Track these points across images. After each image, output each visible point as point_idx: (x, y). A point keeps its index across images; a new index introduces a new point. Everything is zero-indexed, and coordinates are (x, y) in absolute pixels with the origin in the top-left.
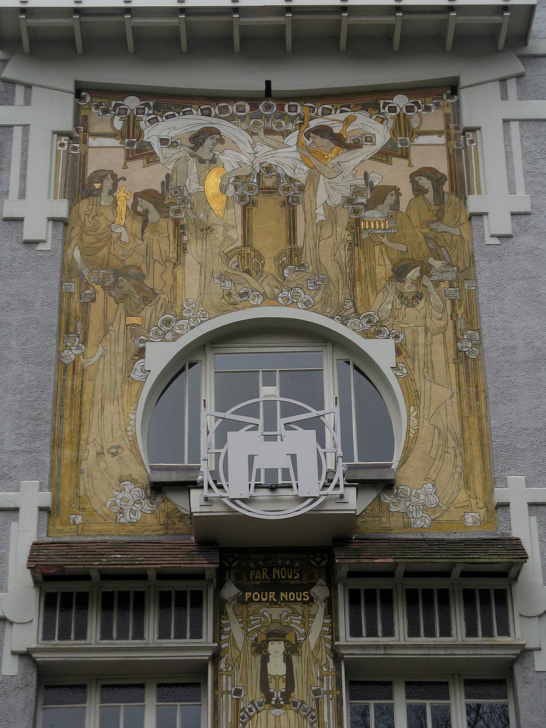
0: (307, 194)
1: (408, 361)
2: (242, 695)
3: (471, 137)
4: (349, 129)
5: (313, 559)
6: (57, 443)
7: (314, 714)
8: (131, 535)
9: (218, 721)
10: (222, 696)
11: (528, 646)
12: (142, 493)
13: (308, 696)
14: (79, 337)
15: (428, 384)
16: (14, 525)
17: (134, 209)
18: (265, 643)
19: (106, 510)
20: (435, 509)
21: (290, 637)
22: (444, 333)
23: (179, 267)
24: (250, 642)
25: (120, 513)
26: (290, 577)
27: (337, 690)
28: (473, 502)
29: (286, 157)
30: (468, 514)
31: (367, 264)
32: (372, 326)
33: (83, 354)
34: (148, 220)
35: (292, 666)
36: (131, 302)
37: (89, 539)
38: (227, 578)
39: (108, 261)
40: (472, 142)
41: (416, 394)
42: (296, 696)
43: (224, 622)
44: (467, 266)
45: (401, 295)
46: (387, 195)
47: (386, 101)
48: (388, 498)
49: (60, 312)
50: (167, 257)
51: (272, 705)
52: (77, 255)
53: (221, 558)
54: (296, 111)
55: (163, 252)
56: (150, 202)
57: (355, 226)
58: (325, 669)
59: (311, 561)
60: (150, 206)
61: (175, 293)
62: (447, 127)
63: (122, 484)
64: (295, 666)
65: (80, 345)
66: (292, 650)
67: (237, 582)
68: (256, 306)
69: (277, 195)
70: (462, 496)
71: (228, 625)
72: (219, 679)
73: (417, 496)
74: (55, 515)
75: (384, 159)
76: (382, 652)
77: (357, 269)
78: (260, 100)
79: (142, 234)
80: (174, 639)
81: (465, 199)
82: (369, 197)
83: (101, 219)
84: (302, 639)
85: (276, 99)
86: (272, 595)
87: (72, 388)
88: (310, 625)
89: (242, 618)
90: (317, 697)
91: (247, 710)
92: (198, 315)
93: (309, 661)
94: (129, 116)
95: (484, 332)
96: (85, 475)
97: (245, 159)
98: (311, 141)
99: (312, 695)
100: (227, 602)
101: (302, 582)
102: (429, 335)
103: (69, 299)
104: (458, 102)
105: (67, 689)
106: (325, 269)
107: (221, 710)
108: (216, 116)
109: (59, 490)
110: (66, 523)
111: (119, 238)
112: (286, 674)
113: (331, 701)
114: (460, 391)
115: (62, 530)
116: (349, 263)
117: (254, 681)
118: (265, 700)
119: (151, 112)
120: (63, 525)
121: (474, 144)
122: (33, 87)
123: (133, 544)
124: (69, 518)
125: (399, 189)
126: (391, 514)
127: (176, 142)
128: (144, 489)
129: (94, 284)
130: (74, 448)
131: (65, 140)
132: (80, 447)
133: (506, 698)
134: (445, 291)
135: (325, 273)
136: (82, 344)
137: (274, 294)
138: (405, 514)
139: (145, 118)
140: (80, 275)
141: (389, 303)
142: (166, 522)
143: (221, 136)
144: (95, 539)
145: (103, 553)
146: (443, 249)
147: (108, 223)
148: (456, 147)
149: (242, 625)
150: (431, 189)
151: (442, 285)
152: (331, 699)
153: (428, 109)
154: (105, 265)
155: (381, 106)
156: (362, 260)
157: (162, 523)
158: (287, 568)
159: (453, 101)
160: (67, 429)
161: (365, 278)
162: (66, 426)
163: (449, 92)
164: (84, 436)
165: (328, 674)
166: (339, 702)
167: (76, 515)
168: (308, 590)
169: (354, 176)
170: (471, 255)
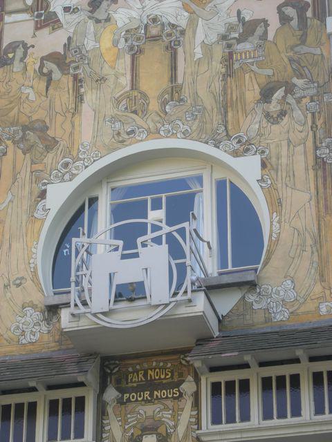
0: (187, 36)
5: (183, 359)
15: (289, 190)
21: (162, 430)
22: (305, 143)
24: (127, 437)
26: (163, 377)
29: (170, 7)
38: (108, 383)
39: (18, 120)
45: (268, 115)
46: (257, 27)
48: (251, 297)
55: (64, 105)
56: (54, 63)
57: (229, 59)
60: (53, 67)
69: (161, 42)
70: (318, 289)
71: (109, 424)
73: (278, 293)
77: (229, 97)
79: (47, 92)
82: (241, 31)
86: (147, 394)
97: (134, 14)
111: (27, 98)
114: (317, 194)
125: (267, 21)
127: (77, 8)
135: (200, 104)
141: (256, 123)
146: (305, 69)
149: (120, 423)
150: (296, 17)
151: (304, 100)
156: (234, 88)
158: (160, 369)
168: (178, 387)
169: (228, 15)
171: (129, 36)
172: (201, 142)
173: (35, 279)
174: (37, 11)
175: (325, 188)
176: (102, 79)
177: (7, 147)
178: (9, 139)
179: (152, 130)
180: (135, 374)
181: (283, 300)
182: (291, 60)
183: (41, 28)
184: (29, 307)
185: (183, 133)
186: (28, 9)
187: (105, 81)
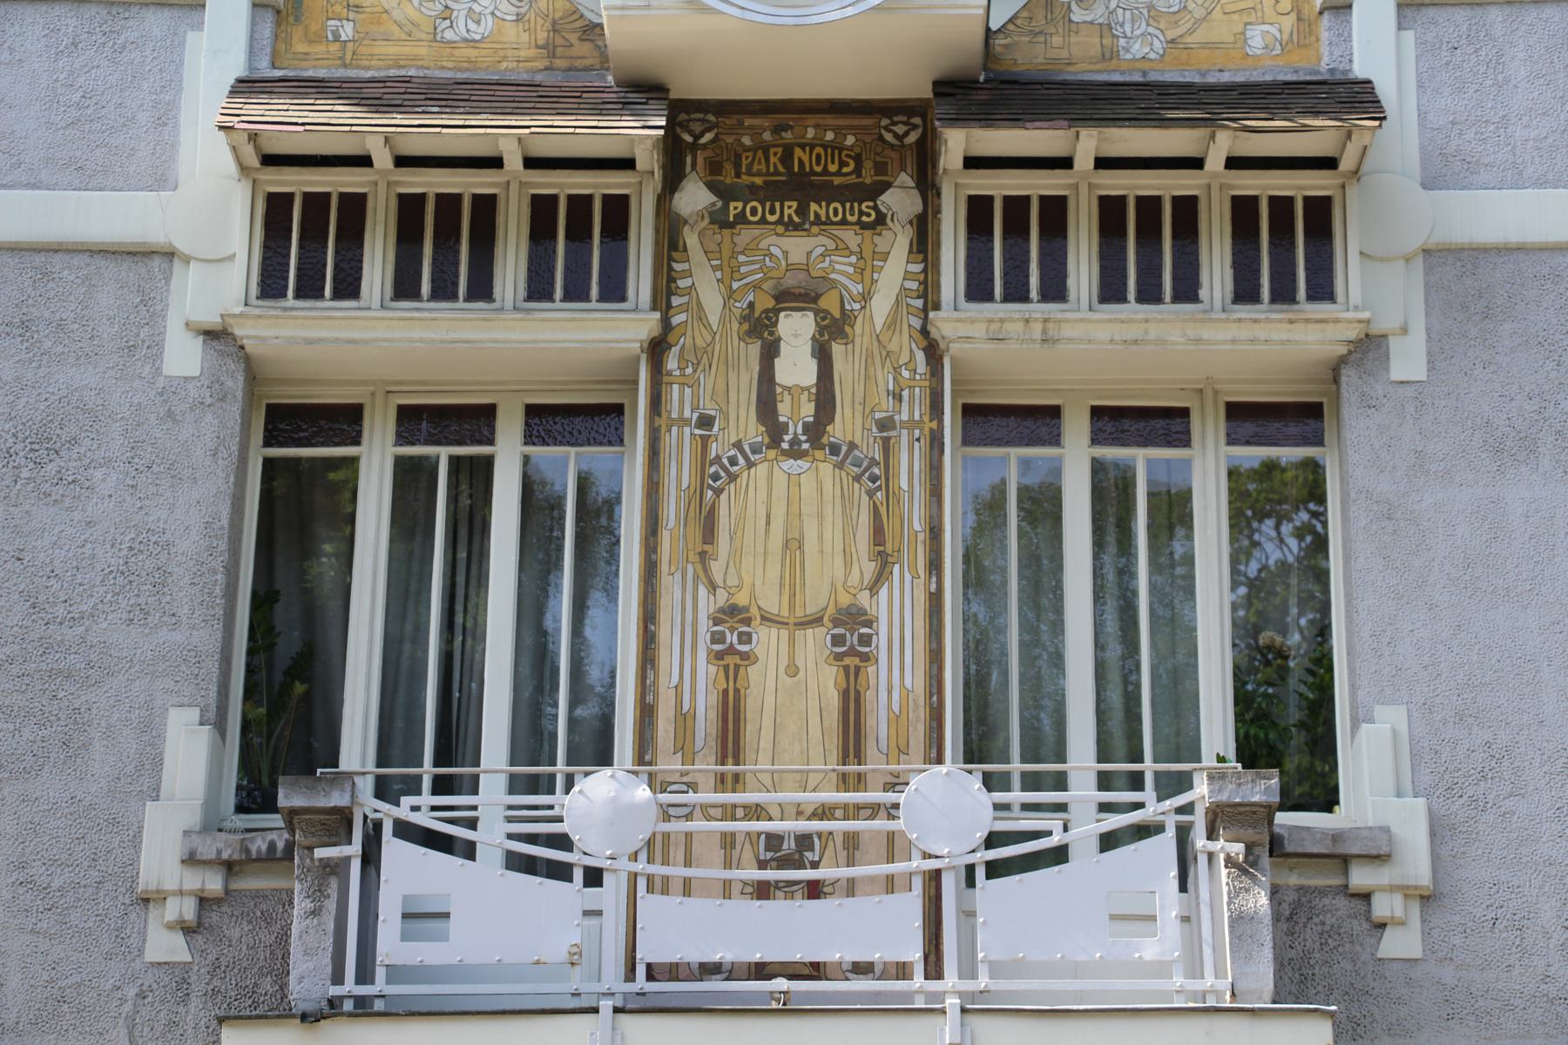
2: (716, 428)
5: (887, 128)
7: (876, 471)
8: (467, 70)
9: (658, 483)
10: (670, 431)
13: (866, 431)
18: (771, 315)
21: (829, 302)
24: (737, 312)
25: (444, 19)
26: (833, 168)
27: (931, 421)
30: (1254, 27)
35: (831, 367)
37: (369, 74)
38: (688, 168)
42: (838, 431)
43: (677, 267)
51: (783, 450)
58: (906, 374)
59: (883, 132)
64: (839, 365)
66: (832, 330)
67: (709, 178)
72: (664, 394)
74: (291, 19)
80: (561, 301)
84: (857, 306)
86: (790, 209)
88: (876, 276)
90: (885, 434)
91: (725, 461)
93: (869, 355)
99: (875, 429)
100: (686, 222)
101: (861, 180)
107: (667, 462)
110: (317, 38)
113: (916, 444)
115: (306, 54)
117: (743, 397)
118: (767, 440)
120: (311, 42)
123: (469, 87)
124: (325, 27)
126: (1073, 27)
138: (1106, 28)
142: (551, 41)
144: (382, 74)
145: (399, 102)
152: (918, 440)
157: (541, 43)
158: (825, 147)
165: (912, 383)
166: (936, 443)
167: (340, 20)
180: (760, 152)
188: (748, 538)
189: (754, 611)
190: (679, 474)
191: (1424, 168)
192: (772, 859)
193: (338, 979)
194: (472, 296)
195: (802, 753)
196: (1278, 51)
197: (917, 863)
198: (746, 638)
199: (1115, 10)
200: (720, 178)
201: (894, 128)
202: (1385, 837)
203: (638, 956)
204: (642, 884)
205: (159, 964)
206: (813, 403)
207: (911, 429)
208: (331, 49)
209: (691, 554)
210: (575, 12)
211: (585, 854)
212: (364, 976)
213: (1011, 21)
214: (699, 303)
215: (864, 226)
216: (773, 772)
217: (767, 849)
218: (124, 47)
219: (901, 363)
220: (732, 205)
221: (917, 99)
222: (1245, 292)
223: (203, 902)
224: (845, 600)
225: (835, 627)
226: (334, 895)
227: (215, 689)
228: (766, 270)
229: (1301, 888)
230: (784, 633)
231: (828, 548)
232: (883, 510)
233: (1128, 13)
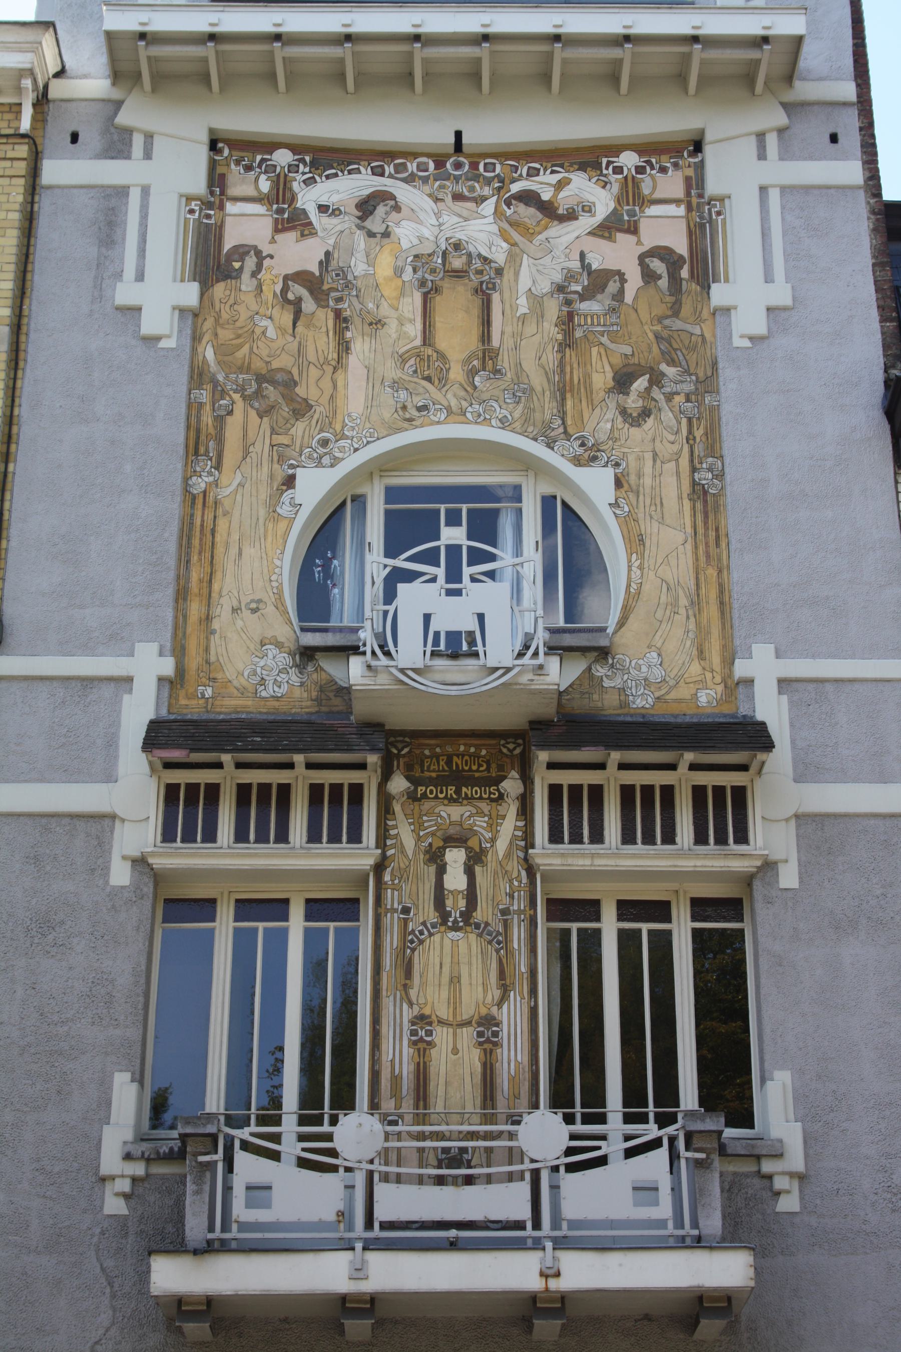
1: (631, 496)
2: (412, 914)
3: (718, 206)
4: (562, 195)
5: (504, 746)
6: (182, 594)
7: (500, 938)
9: (380, 945)
10: (386, 916)
11: (774, 857)
12: (289, 660)
14: (211, 459)
15: (655, 525)
16: (126, 697)
17: (284, 296)
19: (244, 683)
20: (660, 685)
21: (473, 843)
22: (677, 460)
23: (340, 371)
24: (423, 849)
25: (261, 685)
26: (474, 768)
27: (530, 910)
28: (709, 675)
31: (581, 370)
32: (586, 451)
33: (216, 483)
34: (300, 310)
36: (279, 417)
37: (221, 717)
38: (395, 768)
39: (249, 363)
40: (719, 213)
41: (640, 537)
42: (479, 915)
43: (390, 823)
44: (709, 374)
45: (624, 412)
46: (608, 281)
47: (610, 159)
49: (188, 427)
50: (326, 358)
52: (210, 354)
53: (387, 743)
54: (494, 171)
55: (320, 352)
56: (304, 287)
57: (568, 321)
58: (516, 883)
59: (502, 748)
61: (334, 404)
62: (688, 194)
63: (264, 648)
65: (213, 470)
66: (475, 859)
68: (438, 423)
69: (467, 281)
70: (695, 668)
71: (395, 827)
75: (607, 235)
76: (588, 862)
77: (568, 377)
78: (449, 156)
81: (709, 287)
82: (586, 283)
83: (241, 309)
84: (488, 845)
85: (467, 156)
86: (451, 790)
87: (202, 526)
89: (413, 819)
90: (505, 917)
91: (417, 933)
92: (364, 433)
93: (496, 873)
94: (279, 174)
95: (727, 460)
96: (217, 636)
97: (427, 233)
98: (512, 210)
99: (499, 915)
100: (394, 798)
102: (658, 462)
103: (199, 411)
104: (702, 162)
105: (192, 903)
106: (528, 376)
108: (391, 176)
109: (184, 655)
110: (194, 696)
111: (264, 333)
112: (467, 890)
113: (522, 923)
115: (187, 705)
116: (559, 369)
117: (427, 897)
118: (440, 921)
119: (307, 170)
120: (189, 699)
121: (722, 217)
122: (156, 138)
123: (276, 724)
124: (196, 690)
125: (624, 274)
126: (604, 690)
127: (338, 209)
128: (292, 654)
129: (231, 393)
130: (204, 602)
131: (196, 205)
132: (211, 601)
133: (742, 921)
134: (680, 407)
135: (526, 381)
136: (215, 469)
137: (461, 408)
138: (622, 690)
139: (300, 177)
140: (215, 383)
141: (608, 421)
143: (396, 202)
144: (229, 717)
146: (679, 353)
147: (252, 313)
148: (698, 220)
150: (665, 275)
152: (523, 921)
153: (663, 170)
154: (244, 368)
155: (604, 165)
156: (575, 366)
157: (314, 697)
159: (696, 160)
160: (195, 576)
161: (579, 389)
162: (194, 574)
163: (691, 148)
164: (216, 587)
165: (519, 889)
167: (205, 686)
168: (497, 786)
169: (567, 256)
170: (714, 361)
171: (420, 264)
172: (527, 436)
173: (280, 606)
174: (277, 203)
175: (706, 528)
176: (377, 324)
177: (233, 402)
178: (235, 391)
179: (454, 409)
181: (646, 679)
182: (657, 337)
183: (284, 230)
184: (271, 644)
185: (500, 420)
186: (263, 199)
187: (383, 326)
188: (430, 975)
189: (434, 1018)
190: (392, 940)
191: (795, 770)
192: (445, 1158)
193: (211, 1229)
194: (276, 841)
195: (461, 1098)
196: (715, 704)
197: (528, 1165)
198: (429, 1033)
199: (626, 680)
200: (413, 773)
201: (508, 746)
202: (779, 1144)
203: (375, 1216)
204: (376, 1177)
205: (111, 1215)
206: (465, 901)
207: (519, 915)
208: (200, 702)
209: (399, 985)
210: (332, 681)
211: (345, 1160)
212: (225, 1228)
213: (570, 686)
214: (401, 843)
215: (492, 800)
216: (445, 1113)
217: (442, 1153)
218: (90, 703)
219: (513, 877)
220: (419, 788)
221: (520, 730)
222: (701, 838)
223: (135, 1180)
224: (484, 1011)
225: (479, 1027)
226: (208, 1183)
227: (139, 1061)
228: (438, 825)
229: (735, 1174)
230: (451, 1030)
231: (474, 982)
232: (504, 961)
233: (634, 682)
